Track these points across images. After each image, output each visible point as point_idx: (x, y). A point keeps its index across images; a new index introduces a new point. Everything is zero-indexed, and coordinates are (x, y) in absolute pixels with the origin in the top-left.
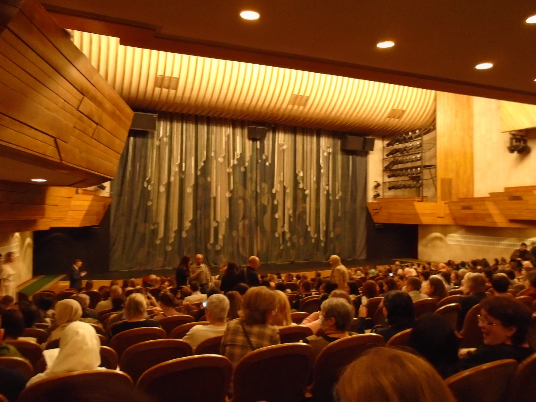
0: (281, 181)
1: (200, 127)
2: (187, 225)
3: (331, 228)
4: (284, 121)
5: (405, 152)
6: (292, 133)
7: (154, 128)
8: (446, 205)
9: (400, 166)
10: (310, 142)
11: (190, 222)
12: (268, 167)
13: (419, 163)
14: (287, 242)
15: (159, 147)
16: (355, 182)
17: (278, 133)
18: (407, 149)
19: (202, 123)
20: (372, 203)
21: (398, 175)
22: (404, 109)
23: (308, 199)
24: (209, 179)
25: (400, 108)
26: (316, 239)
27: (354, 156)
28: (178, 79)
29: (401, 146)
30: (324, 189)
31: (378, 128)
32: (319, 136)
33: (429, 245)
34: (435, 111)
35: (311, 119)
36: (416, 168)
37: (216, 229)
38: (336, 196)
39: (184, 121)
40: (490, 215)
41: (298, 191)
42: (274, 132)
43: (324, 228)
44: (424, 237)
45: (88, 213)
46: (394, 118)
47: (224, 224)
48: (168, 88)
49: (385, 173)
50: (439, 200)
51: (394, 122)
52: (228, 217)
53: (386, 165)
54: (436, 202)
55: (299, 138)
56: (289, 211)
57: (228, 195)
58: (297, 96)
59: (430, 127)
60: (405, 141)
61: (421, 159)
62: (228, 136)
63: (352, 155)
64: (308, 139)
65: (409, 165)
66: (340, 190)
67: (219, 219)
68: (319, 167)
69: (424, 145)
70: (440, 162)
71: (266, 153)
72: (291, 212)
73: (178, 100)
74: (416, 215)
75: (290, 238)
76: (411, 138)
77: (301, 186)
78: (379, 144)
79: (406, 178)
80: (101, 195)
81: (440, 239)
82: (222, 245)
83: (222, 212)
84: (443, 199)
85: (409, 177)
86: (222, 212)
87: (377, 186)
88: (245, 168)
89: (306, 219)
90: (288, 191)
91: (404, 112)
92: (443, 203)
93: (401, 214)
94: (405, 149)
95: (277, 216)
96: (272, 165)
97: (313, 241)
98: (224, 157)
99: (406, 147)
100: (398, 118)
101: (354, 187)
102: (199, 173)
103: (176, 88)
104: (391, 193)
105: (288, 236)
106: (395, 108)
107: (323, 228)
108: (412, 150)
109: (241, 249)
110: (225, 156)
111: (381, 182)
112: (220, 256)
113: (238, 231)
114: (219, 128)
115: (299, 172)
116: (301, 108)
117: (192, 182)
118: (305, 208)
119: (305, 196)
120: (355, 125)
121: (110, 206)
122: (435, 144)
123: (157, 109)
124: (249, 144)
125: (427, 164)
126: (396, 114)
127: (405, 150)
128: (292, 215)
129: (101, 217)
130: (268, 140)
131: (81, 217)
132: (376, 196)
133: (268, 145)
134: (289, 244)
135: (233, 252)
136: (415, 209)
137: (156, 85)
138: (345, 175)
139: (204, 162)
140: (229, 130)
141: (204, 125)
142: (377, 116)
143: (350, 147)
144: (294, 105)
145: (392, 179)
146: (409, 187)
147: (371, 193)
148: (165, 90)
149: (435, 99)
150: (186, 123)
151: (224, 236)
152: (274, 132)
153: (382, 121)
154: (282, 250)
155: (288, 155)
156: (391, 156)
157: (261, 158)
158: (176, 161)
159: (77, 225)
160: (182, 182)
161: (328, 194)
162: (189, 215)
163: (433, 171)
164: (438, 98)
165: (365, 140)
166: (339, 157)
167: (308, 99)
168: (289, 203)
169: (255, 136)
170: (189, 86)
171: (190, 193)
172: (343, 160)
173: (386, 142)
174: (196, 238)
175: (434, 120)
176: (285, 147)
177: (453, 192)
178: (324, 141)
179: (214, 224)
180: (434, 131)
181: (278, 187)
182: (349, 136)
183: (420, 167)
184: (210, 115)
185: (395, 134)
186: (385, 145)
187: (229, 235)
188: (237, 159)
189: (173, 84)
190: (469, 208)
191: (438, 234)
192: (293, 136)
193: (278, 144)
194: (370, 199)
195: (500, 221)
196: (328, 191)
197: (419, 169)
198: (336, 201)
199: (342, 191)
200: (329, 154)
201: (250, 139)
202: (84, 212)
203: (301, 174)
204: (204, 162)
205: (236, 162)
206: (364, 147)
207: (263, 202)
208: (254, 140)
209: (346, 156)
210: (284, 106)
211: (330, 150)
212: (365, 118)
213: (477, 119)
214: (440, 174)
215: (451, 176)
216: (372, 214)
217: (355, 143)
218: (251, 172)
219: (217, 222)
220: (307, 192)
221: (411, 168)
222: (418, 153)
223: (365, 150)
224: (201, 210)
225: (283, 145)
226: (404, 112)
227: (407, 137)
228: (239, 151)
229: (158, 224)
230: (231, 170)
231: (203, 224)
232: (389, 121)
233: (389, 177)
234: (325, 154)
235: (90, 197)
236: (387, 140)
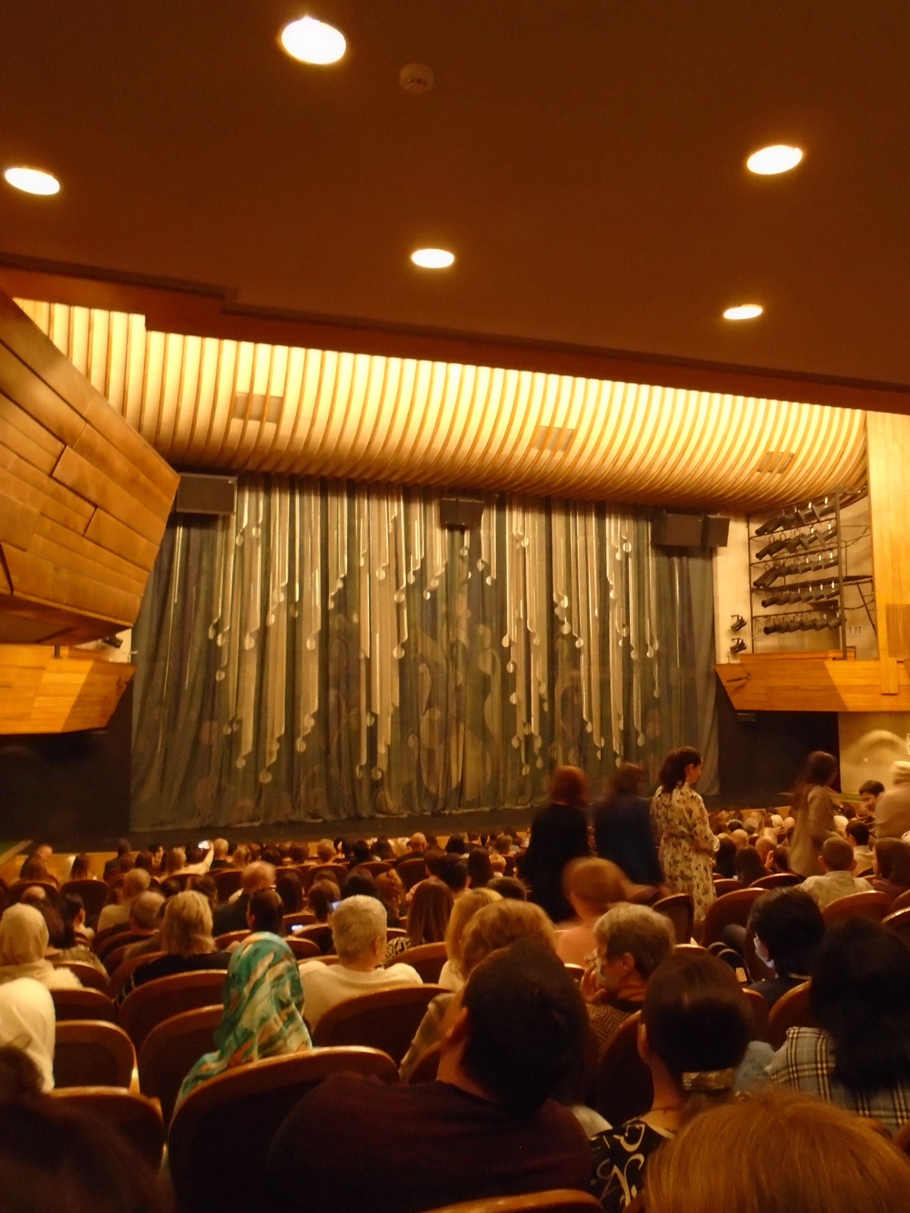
0: (519, 619)
1: (332, 501)
2: (308, 722)
3: (637, 723)
4: (520, 485)
5: (799, 547)
6: (540, 512)
7: (229, 507)
8: (901, 666)
9: (790, 580)
10: (584, 528)
11: (313, 716)
13: (832, 572)
14: (536, 758)
15: (241, 549)
16: (685, 618)
17: (511, 510)
18: (805, 541)
19: (337, 493)
20: (729, 664)
21: (787, 601)
22: (793, 450)
24: (355, 619)
25: (783, 449)
26: (602, 750)
27: (684, 559)
28: (282, 400)
29: (789, 534)
30: (618, 636)
31: (735, 495)
32: (601, 516)
33: (866, 760)
34: (865, 453)
35: (581, 479)
36: (827, 582)
37: (373, 732)
39: (297, 492)
41: (560, 640)
42: (501, 509)
43: (621, 725)
44: (853, 739)
45: (81, 700)
46: (771, 471)
47: (389, 719)
48: (260, 418)
49: (754, 595)
50: (884, 655)
51: (772, 481)
52: (397, 704)
53: (755, 578)
54: (878, 659)
55: (558, 521)
56: (539, 688)
57: (397, 653)
58: (548, 430)
59: (856, 489)
60: (799, 522)
61: (836, 563)
62: (396, 521)
63: (680, 556)
64: (577, 523)
65: (811, 576)
66: (655, 636)
67: (377, 709)
68: (604, 587)
69: (843, 531)
70: (881, 569)
71: (483, 558)
72: (544, 689)
73: (282, 445)
74: (832, 690)
75: (543, 749)
76: (812, 516)
77: (566, 629)
78: (738, 531)
79: (806, 607)
80: (111, 660)
81: (890, 744)
82: (385, 769)
83: (385, 693)
85: (811, 604)
86: (385, 693)
88: (434, 593)
90: (535, 641)
91: (793, 457)
92: (893, 661)
93: (796, 688)
94: (799, 541)
95: (513, 699)
96: (500, 583)
98: (387, 569)
99: (803, 535)
100: (780, 472)
101: (686, 631)
102: (331, 605)
103: (278, 420)
104: (771, 642)
105: (538, 743)
106: (772, 449)
107: (618, 725)
108: (817, 542)
110: (389, 566)
111: (747, 617)
112: (380, 794)
113: (419, 737)
114: (374, 504)
115: (561, 598)
116: (559, 455)
117: (317, 626)
119: (575, 653)
120: (684, 489)
121: (130, 684)
122: (869, 527)
123: (234, 466)
124: (439, 537)
125: (851, 573)
126: (775, 462)
127: (800, 543)
128: (546, 697)
129: (111, 709)
131: (67, 711)
133: (489, 539)
134: (539, 763)
135: (410, 784)
136: (829, 677)
137: (232, 413)
138: (665, 601)
139: (344, 580)
140: (396, 508)
141: (342, 497)
142: (732, 468)
143: (672, 540)
144: (541, 450)
145: (771, 610)
146: (814, 626)
147: (725, 643)
148: (253, 425)
149: (864, 427)
150: (301, 494)
151: (389, 748)
152: (501, 509)
153: (742, 479)
154: (525, 777)
155: (534, 560)
156: (767, 557)
157: (472, 567)
158: (280, 580)
159: (57, 726)
160: (294, 626)
161: (627, 647)
162: (311, 701)
163: (866, 588)
164: (870, 424)
165: (707, 522)
166: (651, 562)
167: (573, 435)
168: (539, 670)
169: (457, 521)
170: (306, 413)
171: (313, 651)
172: (658, 569)
173: (755, 527)
174: (327, 752)
175: (865, 473)
176: (526, 542)
178: (617, 530)
179: (367, 721)
180: (865, 499)
181: (512, 635)
182: (669, 515)
183: (836, 581)
184: (354, 476)
185: (773, 509)
186: (753, 534)
187: (398, 747)
188: (415, 573)
189: (271, 410)
191: (886, 734)
192: (544, 516)
193: (512, 536)
194: (723, 656)
196: (627, 640)
197: (833, 585)
200: (626, 555)
201: (443, 526)
202: (73, 699)
203: (565, 603)
204: (344, 580)
205: (412, 580)
206: (704, 539)
207: (481, 666)
209: (664, 559)
210: (520, 452)
211: (629, 547)
212: (704, 474)
214: (884, 596)
216: (729, 691)
217: (685, 529)
218: (448, 600)
219: (374, 715)
220: (580, 643)
221: (816, 584)
222: (831, 549)
223: (709, 543)
224: (338, 687)
225: (522, 538)
226: (793, 457)
227: (802, 514)
228: (418, 555)
229: (240, 722)
230: (403, 597)
231: (344, 721)
232: (760, 479)
233: (765, 604)
234: (618, 556)
235: (87, 665)
236: (759, 522)
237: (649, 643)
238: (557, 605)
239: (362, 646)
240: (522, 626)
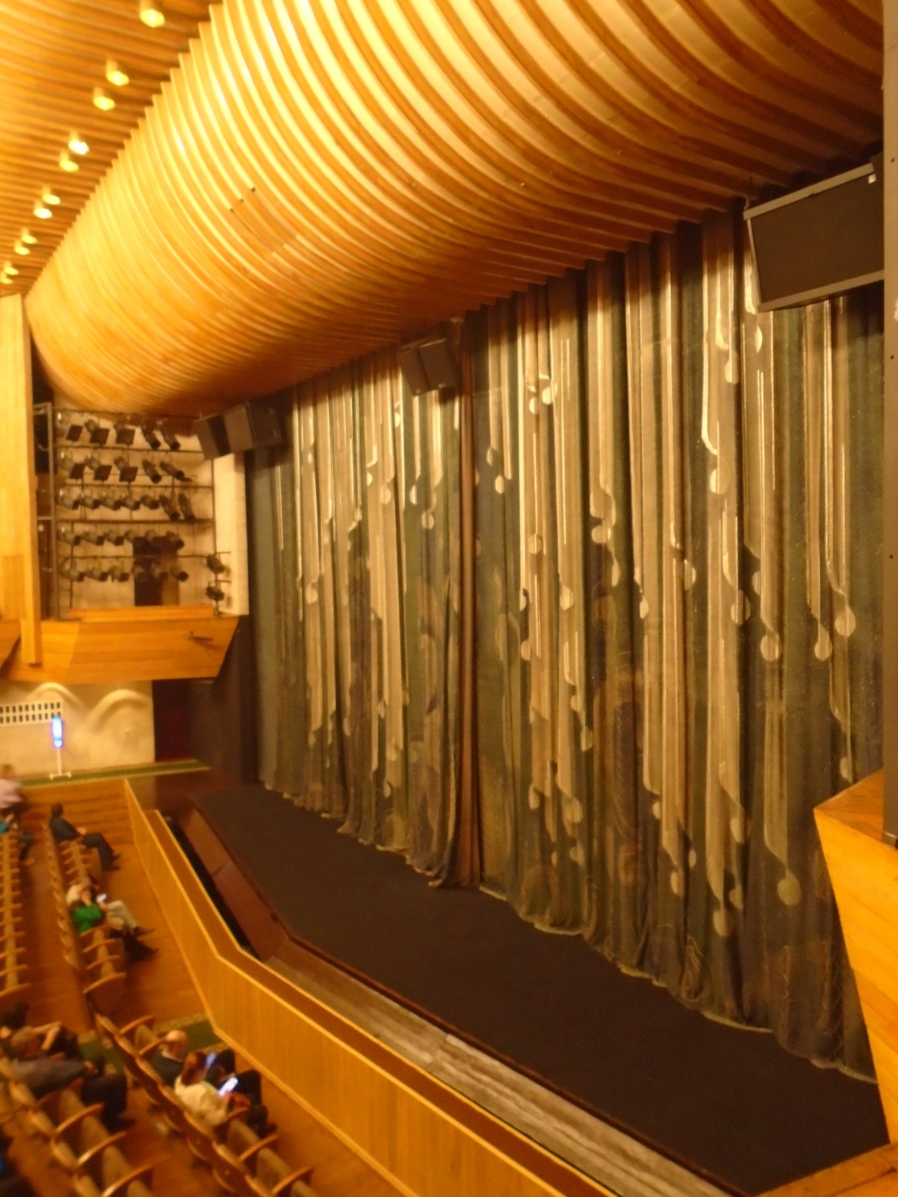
10: (650, 322)
12: (503, 495)
23: (648, 645)
38: (810, 640)
89: (641, 751)
90: (567, 600)
96: (512, 487)
97: (675, 882)
109: (429, 813)
118: (634, 692)
130: (499, 384)
198: (813, 674)
199: (852, 604)
208: (446, 398)
220: (644, 608)
225: (547, 384)
237: (817, 613)
238: (598, 522)
239: (372, 605)
240: (545, 569)
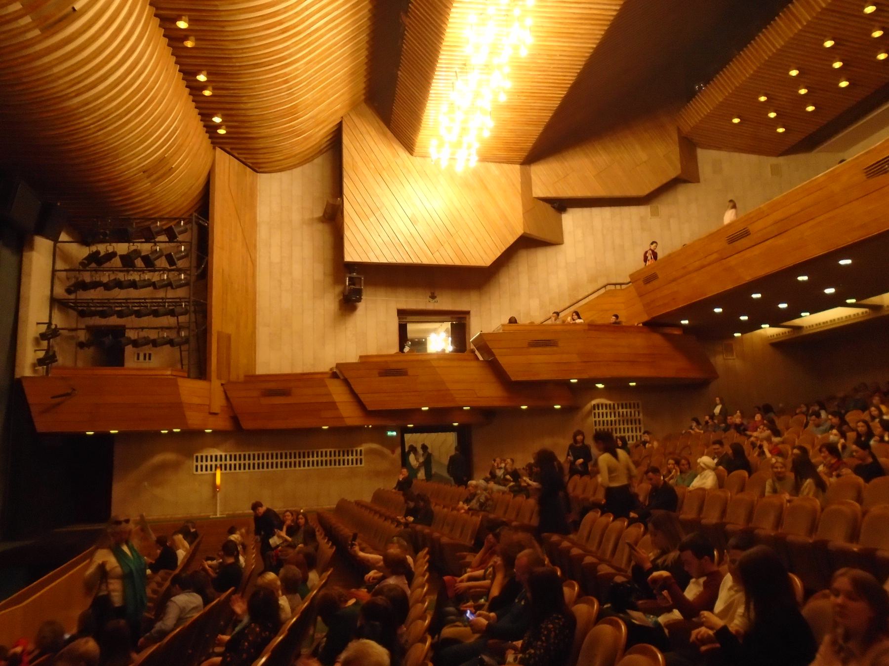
40: (333, 405)
84: (219, 377)
87: (50, 334)
132: (47, 360)
177: (232, 364)
190: (285, 393)
195: (350, 415)
213: (263, 233)
215: (230, 329)
216: (34, 410)
